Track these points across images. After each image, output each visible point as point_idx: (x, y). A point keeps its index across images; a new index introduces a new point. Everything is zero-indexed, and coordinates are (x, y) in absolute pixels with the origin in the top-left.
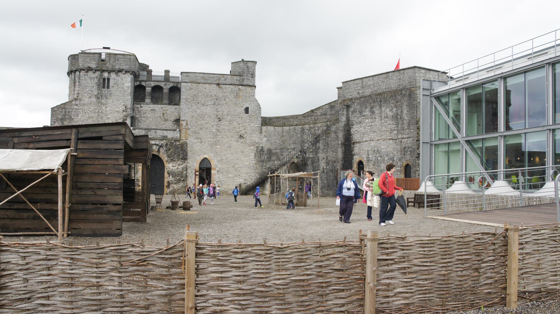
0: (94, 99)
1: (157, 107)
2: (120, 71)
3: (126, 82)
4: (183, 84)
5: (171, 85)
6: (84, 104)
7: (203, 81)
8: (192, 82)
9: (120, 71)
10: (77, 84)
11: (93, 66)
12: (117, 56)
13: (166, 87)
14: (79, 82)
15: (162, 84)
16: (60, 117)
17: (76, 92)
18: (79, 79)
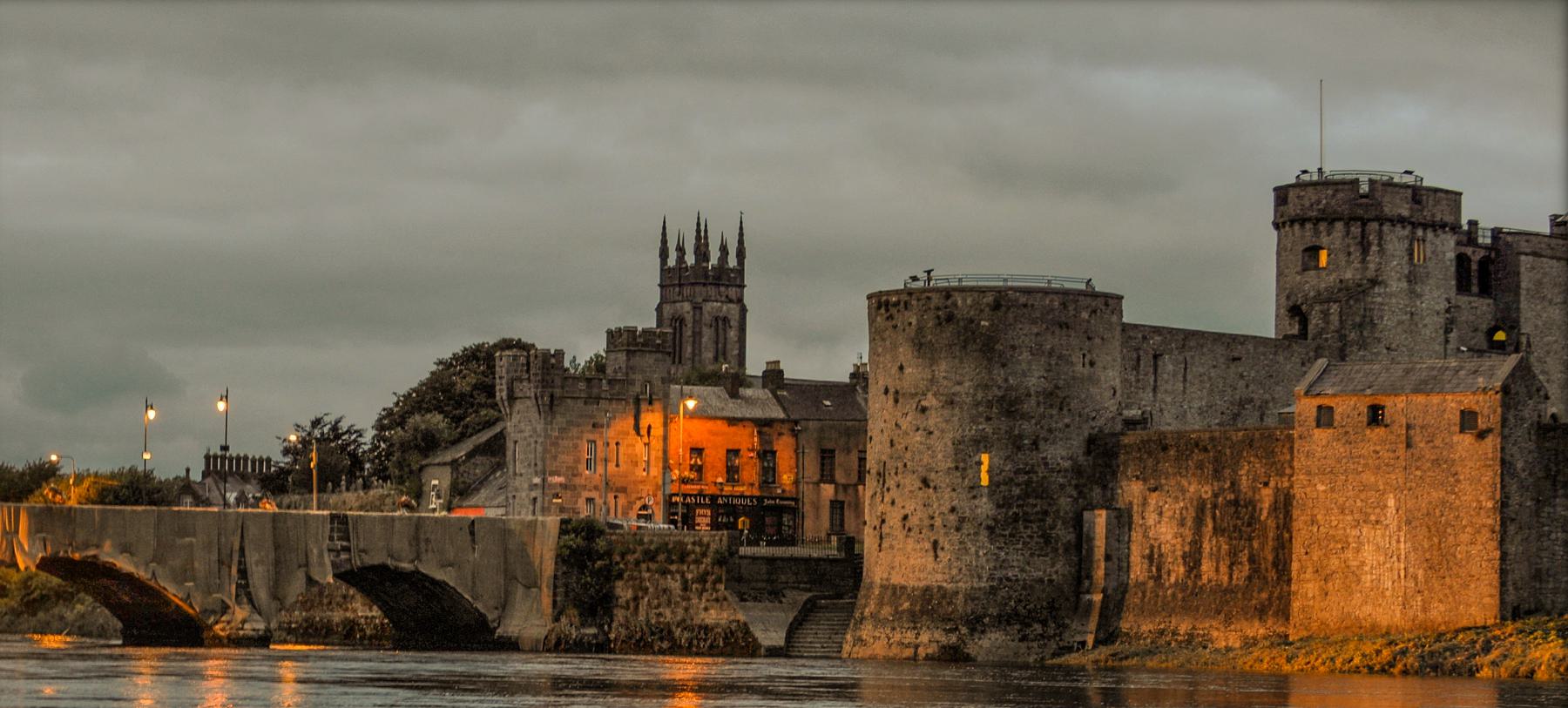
0: (1404, 285)
1: (1463, 300)
2: (1443, 226)
3: (1447, 247)
4: (1523, 258)
5: (1482, 253)
6: (1391, 295)
7: (1549, 252)
8: (1535, 254)
9: (1443, 226)
10: (1374, 248)
11: (1406, 213)
12: (1439, 194)
13: (1476, 256)
14: (1380, 245)
15: (1469, 251)
16: (1358, 320)
17: (1372, 266)
18: (1381, 238)
